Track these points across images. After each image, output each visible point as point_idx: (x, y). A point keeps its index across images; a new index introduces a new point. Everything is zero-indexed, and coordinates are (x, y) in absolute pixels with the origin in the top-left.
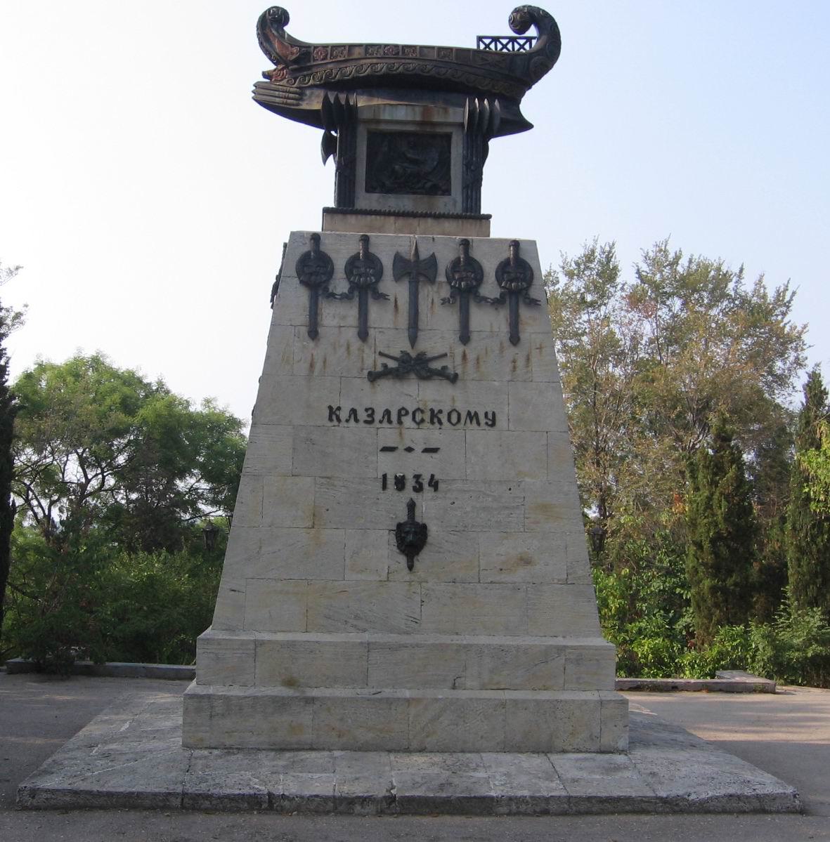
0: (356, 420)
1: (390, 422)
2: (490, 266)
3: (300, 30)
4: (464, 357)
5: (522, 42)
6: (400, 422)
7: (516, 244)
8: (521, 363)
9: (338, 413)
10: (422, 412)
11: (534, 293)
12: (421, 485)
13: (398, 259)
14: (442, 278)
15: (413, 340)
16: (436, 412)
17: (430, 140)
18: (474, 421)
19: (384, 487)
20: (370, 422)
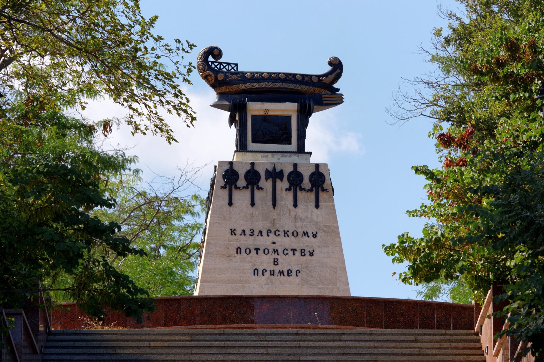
2: (306, 173)
7: (317, 166)
11: (325, 186)
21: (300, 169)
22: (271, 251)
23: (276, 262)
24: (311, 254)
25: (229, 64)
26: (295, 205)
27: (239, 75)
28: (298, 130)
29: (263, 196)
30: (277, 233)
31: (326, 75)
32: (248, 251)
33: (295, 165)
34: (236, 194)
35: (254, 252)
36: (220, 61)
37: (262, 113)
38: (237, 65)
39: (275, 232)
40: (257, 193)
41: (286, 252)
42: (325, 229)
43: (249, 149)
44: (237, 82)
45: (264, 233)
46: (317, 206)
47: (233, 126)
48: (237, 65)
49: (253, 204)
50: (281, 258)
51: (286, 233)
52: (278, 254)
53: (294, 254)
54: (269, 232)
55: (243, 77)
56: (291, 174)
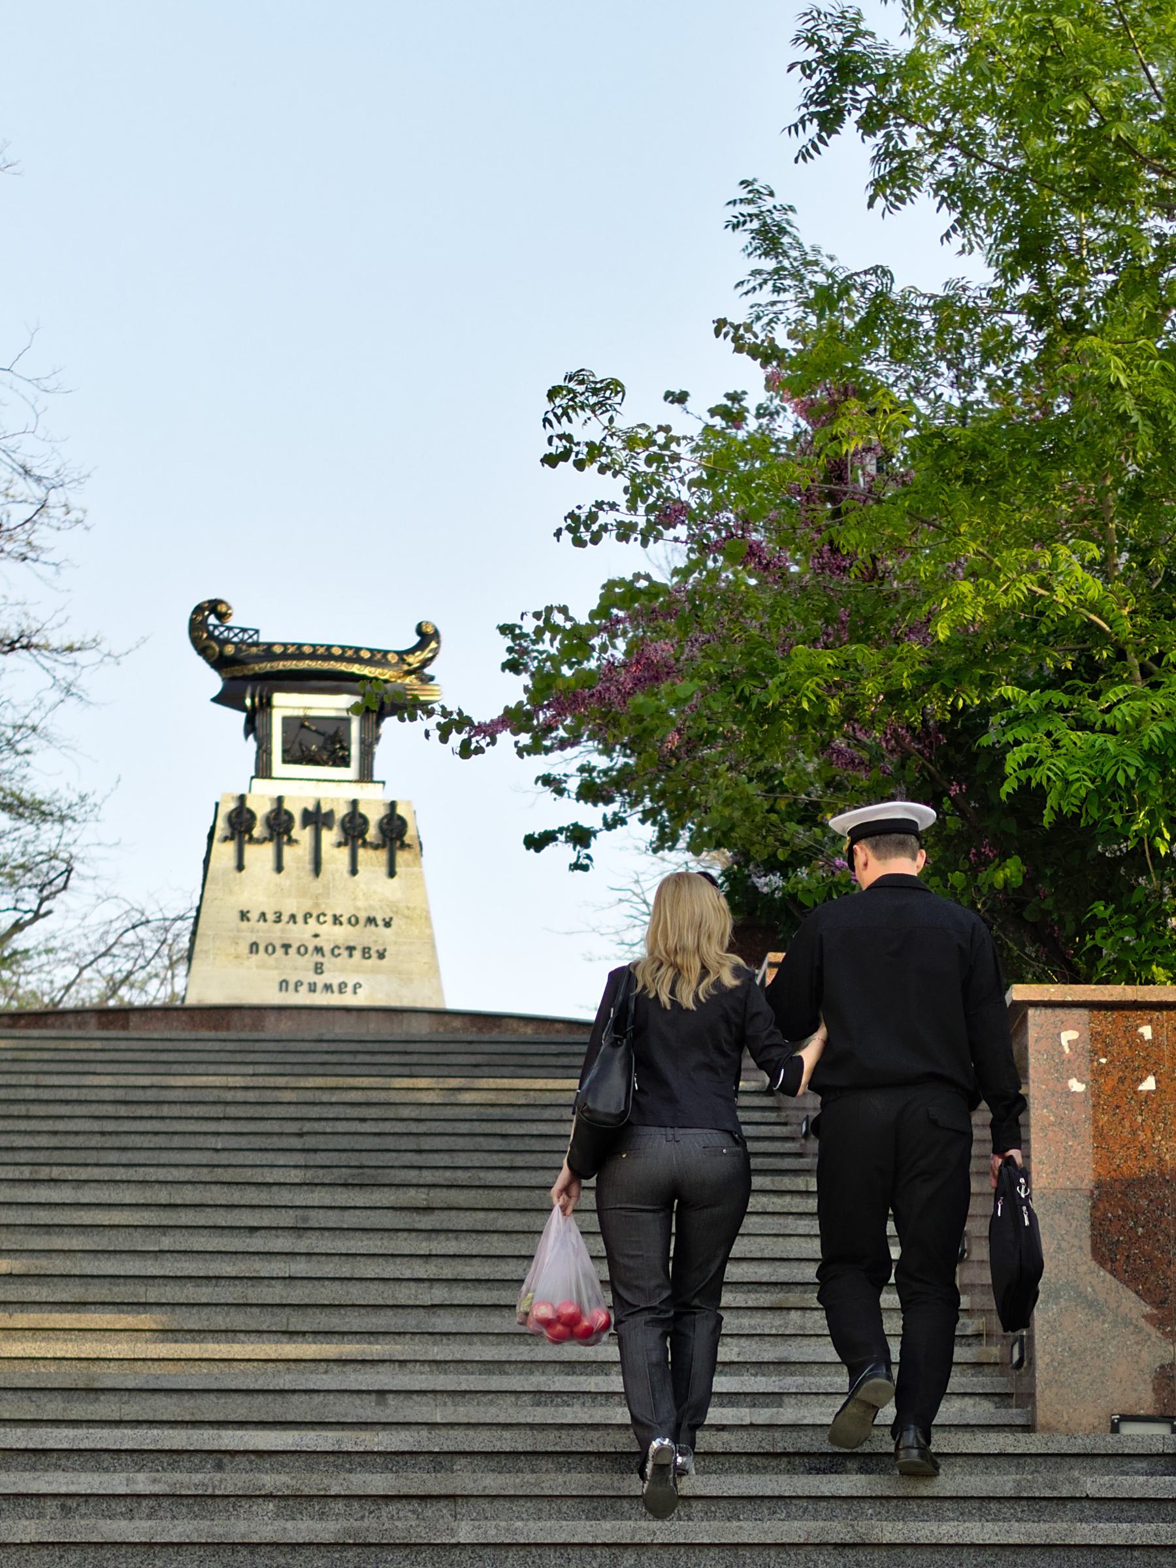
13: (306, 814)
21: (362, 809)
22: (311, 948)
23: (318, 969)
24: (381, 956)
25: (244, 630)
26: (354, 871)
27: (261, 648)
28: (362, 742)
29: (297, 855)
30: (322, 919)
31: (411, 651)
32: (270, 949)
34: (252, 852)
35: (280, 952)
36: (230, 623)
37: (301, 713)
38: (257, 632)
39: (318, 917)
40: (287, 850)
41: (336, 952)
42: (406, 912)
43: (274, 774)
44: (258, 659)
45: (300, 919)
46: (392, 873)
47: (251, 737)
48: (257, 632)
49: (279, 868)
50: (328, 961)
51: (336, 920)
52: (323, 955)
53: (351, 956)
54: (307, 916)
55: (268, 652)
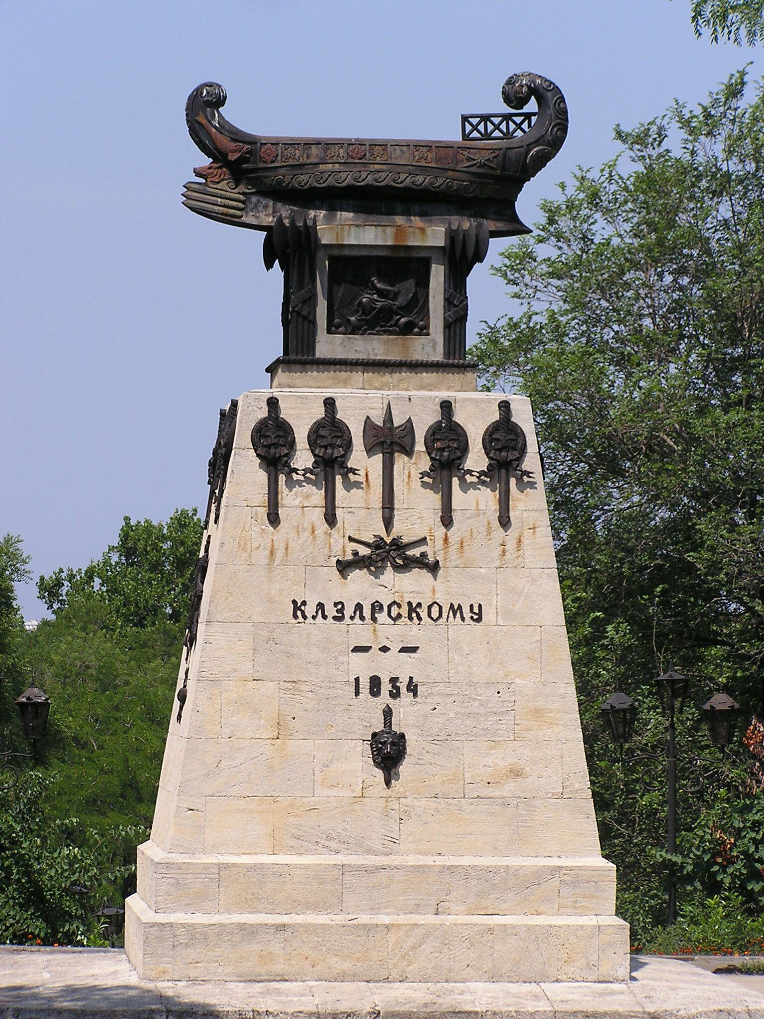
0: (325, 617)
1: (362, 618)
3: (244, 115)
4: (446, 539)
5: (518, 120)
6: (374, 619)
8: (511, 545)
9: (303, 608)
10: (399, 606)
12: (398, 689)
14: (420, 446)
15: (388, 523)
16: (414, 605)
17: (407, 266)
18: (458, 615)
19: (357, 693)
20: (339, 619)
33: (446, 407)
56: (434, 433)
